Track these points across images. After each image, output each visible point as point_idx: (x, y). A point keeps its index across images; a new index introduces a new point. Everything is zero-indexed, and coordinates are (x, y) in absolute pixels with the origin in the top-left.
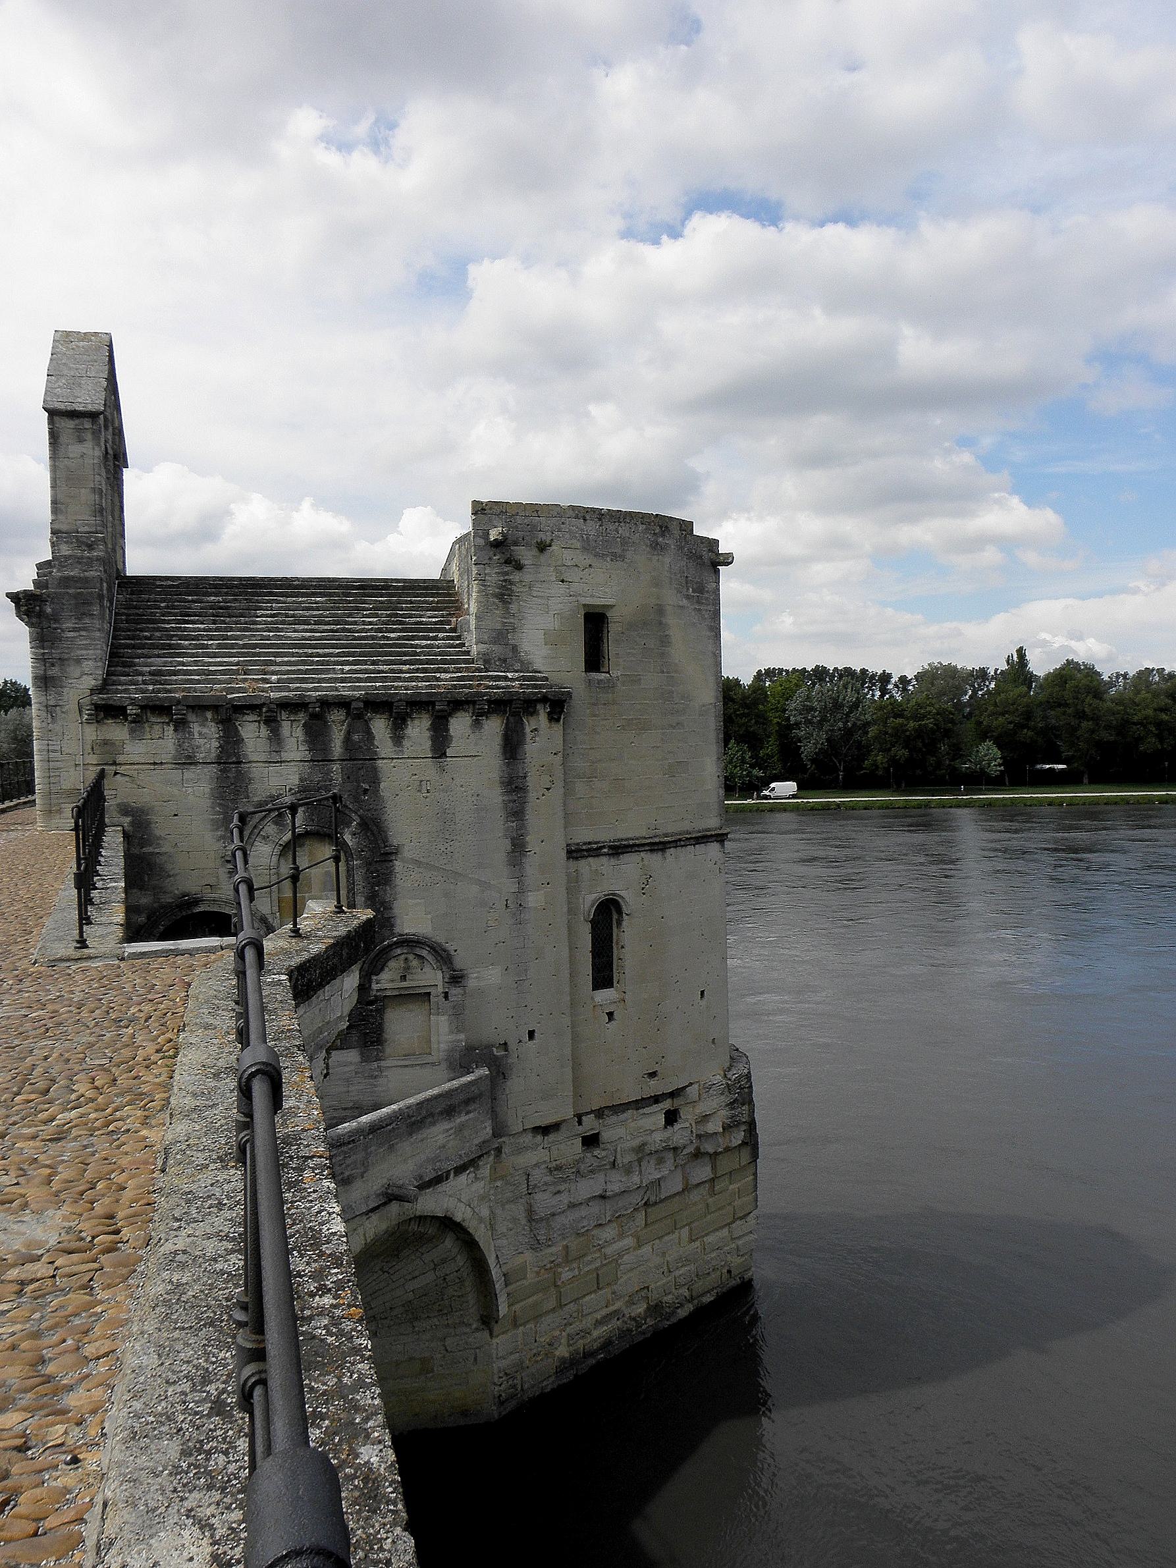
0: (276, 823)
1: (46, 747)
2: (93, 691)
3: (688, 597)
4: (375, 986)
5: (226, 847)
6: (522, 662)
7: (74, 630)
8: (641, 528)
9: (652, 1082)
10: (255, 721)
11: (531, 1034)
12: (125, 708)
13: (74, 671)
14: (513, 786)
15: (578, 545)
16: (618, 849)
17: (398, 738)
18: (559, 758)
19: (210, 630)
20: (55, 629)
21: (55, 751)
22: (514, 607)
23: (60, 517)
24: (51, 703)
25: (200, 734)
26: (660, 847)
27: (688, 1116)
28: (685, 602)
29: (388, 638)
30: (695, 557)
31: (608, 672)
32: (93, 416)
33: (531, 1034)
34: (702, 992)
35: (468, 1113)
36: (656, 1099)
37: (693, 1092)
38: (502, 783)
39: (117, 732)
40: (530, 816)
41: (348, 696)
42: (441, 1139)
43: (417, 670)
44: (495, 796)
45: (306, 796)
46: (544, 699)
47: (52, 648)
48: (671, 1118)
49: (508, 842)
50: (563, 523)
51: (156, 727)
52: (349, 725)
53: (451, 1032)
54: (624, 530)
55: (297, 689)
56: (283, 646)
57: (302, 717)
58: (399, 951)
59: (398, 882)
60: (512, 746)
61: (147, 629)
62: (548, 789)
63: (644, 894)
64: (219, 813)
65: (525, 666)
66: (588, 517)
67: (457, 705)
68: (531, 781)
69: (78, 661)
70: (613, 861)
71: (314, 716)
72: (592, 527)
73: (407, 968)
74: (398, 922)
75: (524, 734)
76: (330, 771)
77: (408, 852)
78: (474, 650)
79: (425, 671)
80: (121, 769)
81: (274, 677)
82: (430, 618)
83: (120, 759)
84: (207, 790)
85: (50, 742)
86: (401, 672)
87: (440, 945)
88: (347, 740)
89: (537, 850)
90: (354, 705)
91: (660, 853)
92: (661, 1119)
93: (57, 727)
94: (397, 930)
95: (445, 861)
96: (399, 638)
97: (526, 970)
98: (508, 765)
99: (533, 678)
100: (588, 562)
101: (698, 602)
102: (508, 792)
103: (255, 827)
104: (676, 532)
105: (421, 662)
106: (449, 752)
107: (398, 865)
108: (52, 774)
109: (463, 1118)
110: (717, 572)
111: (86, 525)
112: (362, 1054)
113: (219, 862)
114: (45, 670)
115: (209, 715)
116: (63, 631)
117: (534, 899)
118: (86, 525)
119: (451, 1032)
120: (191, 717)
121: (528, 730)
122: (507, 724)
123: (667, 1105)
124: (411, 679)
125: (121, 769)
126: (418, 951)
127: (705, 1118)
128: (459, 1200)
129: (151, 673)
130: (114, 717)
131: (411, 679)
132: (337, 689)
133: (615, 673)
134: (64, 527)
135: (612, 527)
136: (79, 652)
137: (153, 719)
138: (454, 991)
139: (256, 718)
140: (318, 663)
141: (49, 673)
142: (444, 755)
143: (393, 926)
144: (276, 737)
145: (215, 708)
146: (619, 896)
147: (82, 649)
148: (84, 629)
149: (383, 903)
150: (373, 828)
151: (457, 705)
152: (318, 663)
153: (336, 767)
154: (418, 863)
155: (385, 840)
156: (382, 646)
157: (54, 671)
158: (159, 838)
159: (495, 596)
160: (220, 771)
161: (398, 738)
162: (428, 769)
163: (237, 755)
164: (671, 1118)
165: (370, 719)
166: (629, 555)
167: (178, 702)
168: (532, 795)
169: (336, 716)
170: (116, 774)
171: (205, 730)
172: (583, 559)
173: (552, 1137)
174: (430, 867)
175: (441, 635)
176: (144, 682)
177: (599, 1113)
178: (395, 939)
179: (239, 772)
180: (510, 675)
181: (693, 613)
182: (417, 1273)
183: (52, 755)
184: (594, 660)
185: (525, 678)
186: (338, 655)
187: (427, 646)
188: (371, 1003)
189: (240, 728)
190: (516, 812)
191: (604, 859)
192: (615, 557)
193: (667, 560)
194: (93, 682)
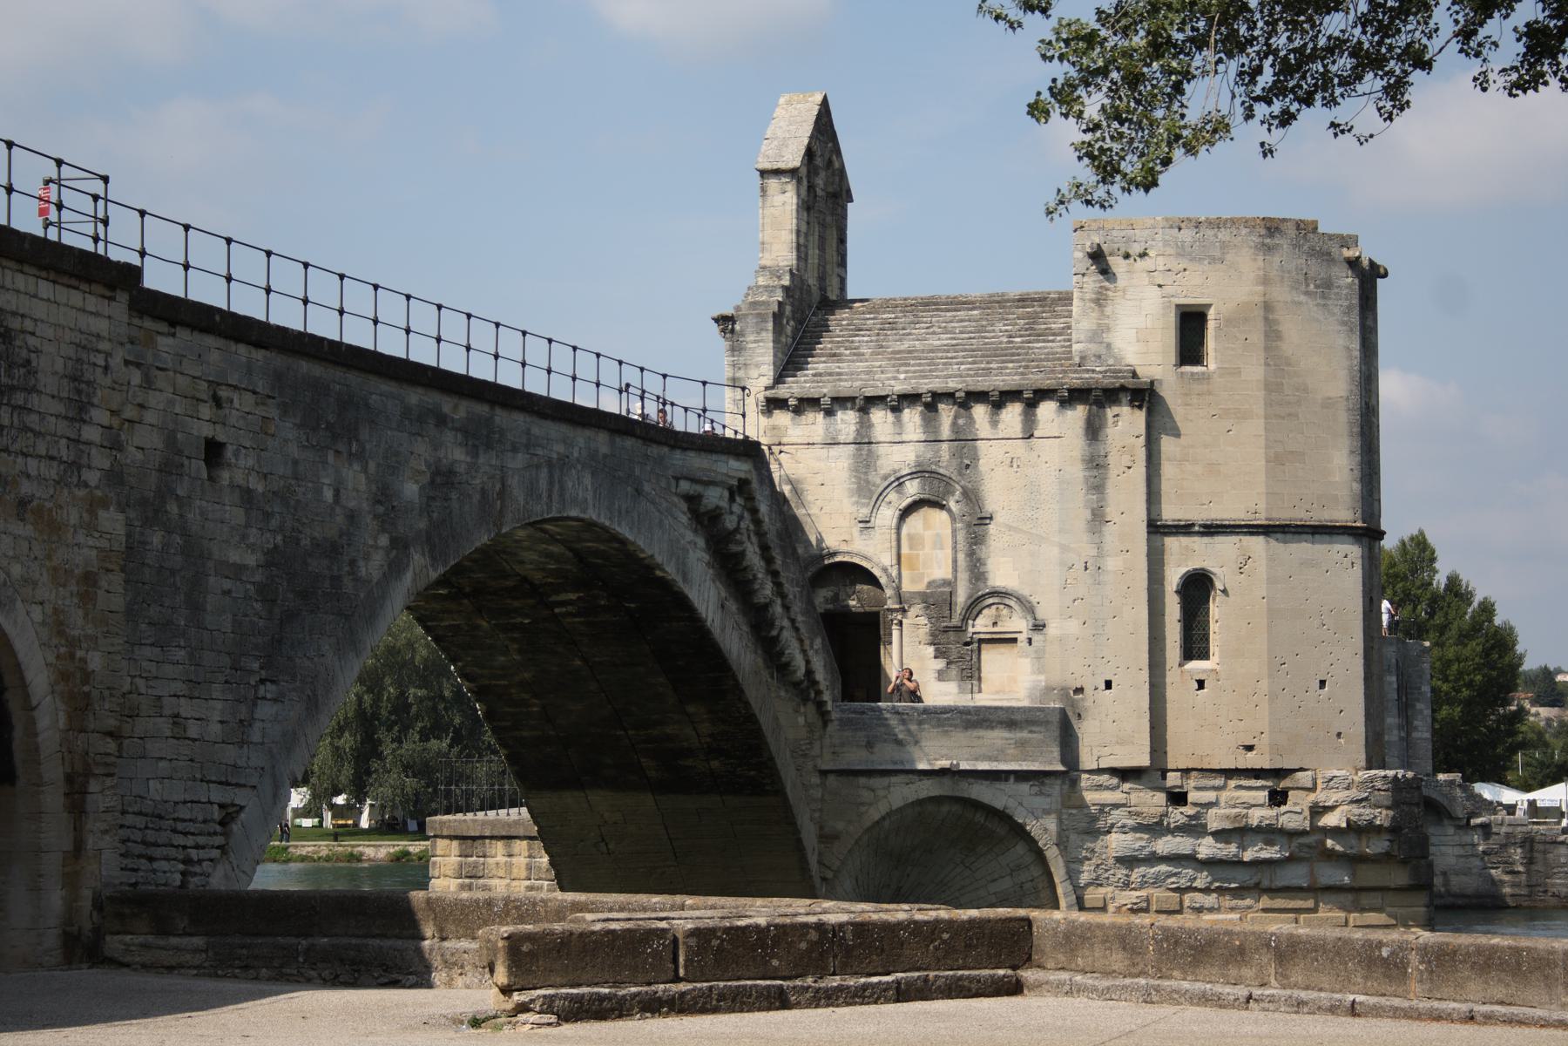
0: (898, 492)
2: (767, 388)
3: (1307, 293)
4: (971, 630)
6: (1116, 358)
7: (755, 342)
8: (1244, 231)
9: (1250, 754)
11: (1108, 685)
13: (754, 373)
15: (1172, 251)
16: (1212, 530)
17: (994, 423)
22: (1108, 310)
25: (842, 420)
27: (1299, 803)
28: (1303, 298)
33: (1108, 685)
35: (1031, 732)
37: (1304, 778)
38: (1083, 460)
39: (782, 418)
40: (1110, 490)
42: (999, 742)
44: (1077, 472)
45: (922, 472)
48: (1278, 798)
52: (956, 412)
53: (1033, 673)
54: (1224, 235)
58: (991, 601)
59: (992, 543)
60: (1093, 430)
62: (1129, 468)
64: (853, 483)
67: (1042, 394)
68: (1111, 459)
69: (758, 366)
70: (1206, 539)
73: (998, 616)
75: (1106, 419)
76: (939, 450)
77: (999, 518)
80: (784, 448)
83: (784, 440)
84: (846, 465)
87: (1025, 598)
88: (954, 424)
89: (1115, 520)
90: (957, 395)
92: (1263, 796)
96: (1022, 342)
98: (1090, 445)
100: (1181, 267)
101: (1324, 296)
103: (881, 494)
104: (1292, 232)
106: (1036, 434)
107: (992, 528)
109: (1025, 734)
112: (959, 686)
113: (854, 522)
115: (849, 405)
117: (1112, 564)
119: (1033, 673)
125: (783, 448)
126: (1007, 601)
128: (1021, 804)
133: (1212, 366)
135: (1210, 233)
138: (1036, 637)
141: (737, 375)
143: (986, 579)
144: (899, 422)
146: (1215, 574)
149: (979, 560)
150: (972, 497)
151: (1042, 394)
154: (1010, 528)
157: (740, 374)
159: (1093, 301)
161: (994, 423)
163: (869, 437)
164: (1278, 798)
166: (1229, 257)
170: (781, 452)
172: (1177, 265)
174: (1016, 530)
177: (1186, 772)
179: (869, 450)
181: (1315, 308)
182: (996, 876)
188: (967, 644)
190: (1097, 487)
191: (1196, 539)
192: (1213, 260)
193: (1277, 259)
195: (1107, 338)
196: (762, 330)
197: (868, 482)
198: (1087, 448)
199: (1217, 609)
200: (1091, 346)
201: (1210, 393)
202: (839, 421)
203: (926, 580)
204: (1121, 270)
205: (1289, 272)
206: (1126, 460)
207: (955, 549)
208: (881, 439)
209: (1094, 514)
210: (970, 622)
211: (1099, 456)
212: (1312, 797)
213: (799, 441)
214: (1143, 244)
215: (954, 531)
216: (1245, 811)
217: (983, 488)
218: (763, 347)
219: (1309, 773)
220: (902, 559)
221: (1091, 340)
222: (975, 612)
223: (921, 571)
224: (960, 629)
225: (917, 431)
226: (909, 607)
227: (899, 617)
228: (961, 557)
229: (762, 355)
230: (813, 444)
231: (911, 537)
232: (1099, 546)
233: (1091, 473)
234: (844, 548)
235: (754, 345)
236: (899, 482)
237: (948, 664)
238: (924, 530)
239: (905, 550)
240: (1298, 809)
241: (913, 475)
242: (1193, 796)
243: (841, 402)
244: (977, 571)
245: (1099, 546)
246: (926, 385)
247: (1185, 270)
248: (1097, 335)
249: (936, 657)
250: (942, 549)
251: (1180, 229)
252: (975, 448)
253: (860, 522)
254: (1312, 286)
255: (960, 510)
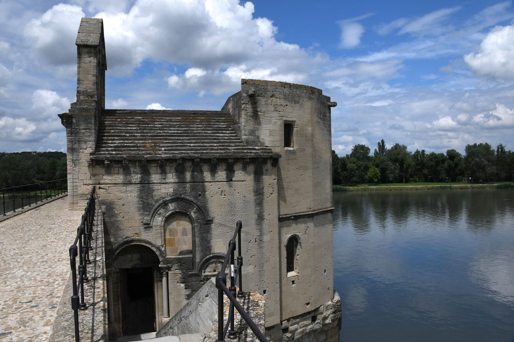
1: (72, 177)
2: (91, 154)
3: (321, 118)
4: (203, 274)
5: (143, 218)
6: (261, 143)
7: (84, 129)
8: (305, 91)
10: (156, 166)
12: (103, 161)
14: (258, 193)
15: (282, 97)
18: (276, 181)
19: (137, 130)
20: (77, 129)
21: (75, 179)
23: (81, 86)
24: (74, 159)
25: (134, 172)
26: (312, 216)
27: (320, 317)
28: (320, 120)
29: (207, 133)
30: (323, 103)
31: (293, 147)
32: (94, 47)
34: (325, 270)
36: (309, 313)
38: (254, 191)
39: (100, 170)
40: (265, 205)
41: (193, 156)
43: (220, 146)
44: (251, 197)
45: (176, 199)
46: (271, 158)
47: (75, 137)
49: (256, 215)
50: (277, 88)
51: (116, 169)
54: (298, 92)
55: (172, 153)
56: (167, 136)
57: (174, 165)
59: (213, 232)
61: (113, 129)
62: (272, 194)
63: (306, 234)
65: (262, 144)
66: (286, 87)
68: (265, 190)
69: (86, 142)
71: (179, 165)
72: (287, 90)
74: (213, 248)
76: (185, 187)
77: (216, 221)
78: (244, 137)
79: (223, 146)
80: (102, 186)
81: (163, 149)
82: (223, 125)
83: (102, 182)
85: (74, 175)
86: (214, 146)
89: (267, 218)
90: (195, 160)
91: (311, 218)
93: (77, 169)
94: (212, 252)
95: (232, 223)
96: (212, 133)
97: (263, 267)
98: (256, 184)
99: (266, 150)
100: (285, 104)
101: (324, 120)
102: (256, 195)
103: (156, 210)
105: (221, 142)
106: (234, 179)
107: (213, 226)
108: (74, 188)
110: (330, 109)
111: (91, 89)
114: (72, 146)
116: (80, 129)
117: (266, 238)
118: (91, 89)
120: (130, 165)
121: (264, 170)
122: (256, 168)
123: (312, 315)
124: (218, 149)
125: (102, 186)
127: (325, 318)
129: (114, 147)
130: (99, 165)
131: (218, 149)
132: (188, 153)
134: (82, 90)
136: (86, 138)
137: (115, 166)
139: (156, 165)
140: (180, 143)
141: (74, 147)
142: (231, 180)
143: (210, 250)
145: (140, 161)
147: (87, 137)
148: (87, 129)
150: (203, 210)
151: (237, 160)
152: (180, 143)
153: (188, 185)
154: (221, 225)
155: (208, 215)
156: (204, 136)
157: (76, 146)
158: (117, 214)
160: (142, 187)
162: (225, 186)
163: (149, 181)
164: (314, 319)
165: (202, 166)
166: (300, 101)
167: (125, 159)
168: (266, 195)
169: (188, 164)
171: (135, 170)
173: (272, 331)
175: (228, 132)
176: (112, 150)
177: (288, 320)
178: (211, 255)
179: (149, 187)
180: (257, 148)
181: (322, 125)
183: (74, 180)
184: (287, 142)
185: (262, 149)
186: (188, 140)
187: (223, 136)
189: (150, 169)
190: (259, 203)
194: (91, 151)
195: (257, 133)
196: (89, 123)
197: (148, 204)
198: (255, 185)
199: (299, 251)
200: (250, 137)
201: (295, 159)
202: (132, 172)
203: (179, 251)
204: (263, 103)
205: (316, 109)
206: (270, 190)
207: (194, 235)
208: (155, 182)
209: (258, 216)
210: (203, 271)
211: (260, 189)
212: (323, 316)
213: (110, 182)
214: (271, 92)
215: (193, 229)
216: (305, 328)
217: (208, 205)
218: (89, 132)
219: (322, 306)
220: (166, 241)
221: (250, 134)
222: (205, 266)
223: (176, 247)
224: (198, 275)
225: (174, 177)
226: (172, 266)
227: (167, 271)
228: (197, 240)
229: (89, 136)
230: (118, 184)
231: (171, 231)
232: (261, 230)
233: (257, 197)
234: (136, 237)
235: (83, 131)
236: (165, 204)
237: (192, 291)
238: (177, 226)
239: (168, 237)
240: (319, 321)
241: (172, 201)
242: (291, 328)
243: (133, 161)
244: (206, 246)
245: (261, 230)
246: (178, 154)
247: (287, 105)
248: (252, 132)
249: (186, 289)
250: (186, 235)
251: (285, 88)
252: (204, 187)
253: (144, 224)
254: (322, 116)
255: (197, 217)
